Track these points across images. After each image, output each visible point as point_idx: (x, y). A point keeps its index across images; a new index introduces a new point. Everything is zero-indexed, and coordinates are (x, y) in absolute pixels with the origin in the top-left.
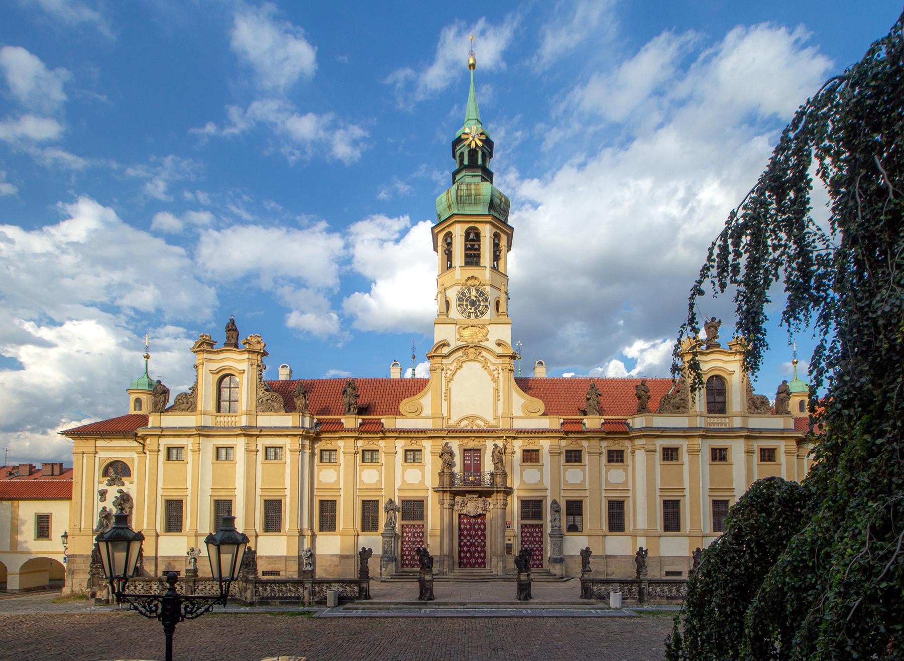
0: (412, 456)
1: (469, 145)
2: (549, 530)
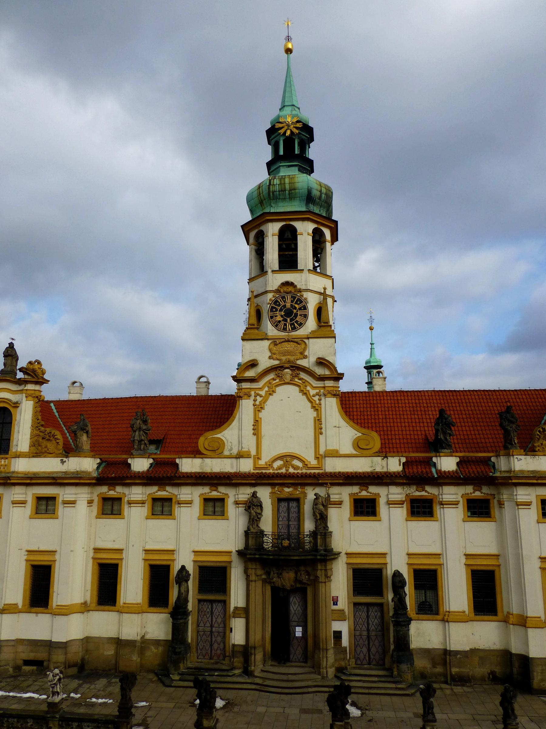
0: (214, 508)
1: (285, 133)
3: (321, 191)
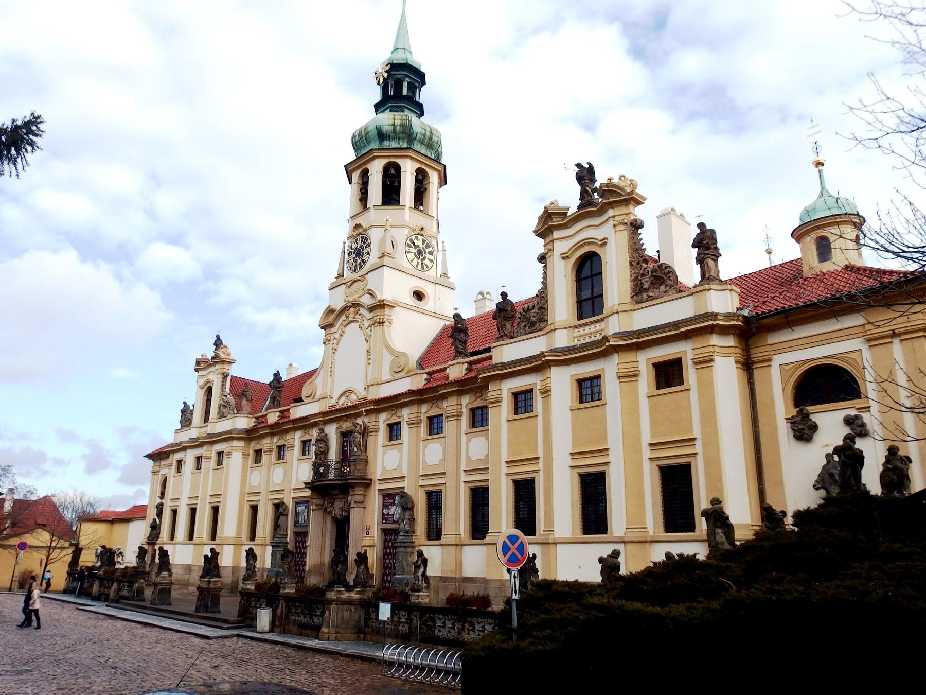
3: (394, 125)
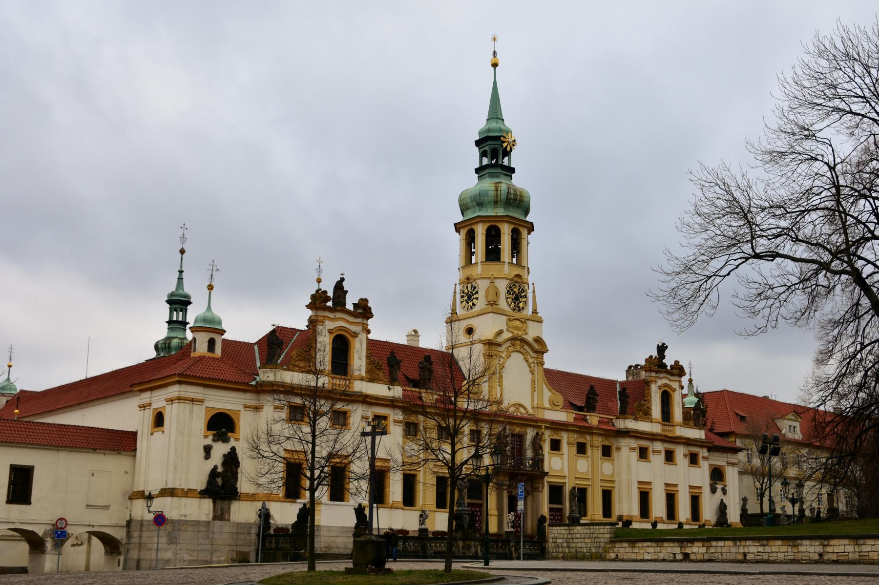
2: (567, 515)
